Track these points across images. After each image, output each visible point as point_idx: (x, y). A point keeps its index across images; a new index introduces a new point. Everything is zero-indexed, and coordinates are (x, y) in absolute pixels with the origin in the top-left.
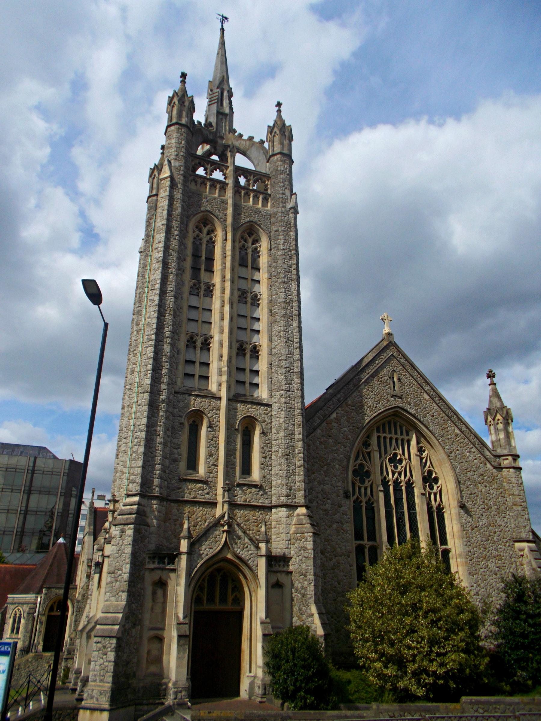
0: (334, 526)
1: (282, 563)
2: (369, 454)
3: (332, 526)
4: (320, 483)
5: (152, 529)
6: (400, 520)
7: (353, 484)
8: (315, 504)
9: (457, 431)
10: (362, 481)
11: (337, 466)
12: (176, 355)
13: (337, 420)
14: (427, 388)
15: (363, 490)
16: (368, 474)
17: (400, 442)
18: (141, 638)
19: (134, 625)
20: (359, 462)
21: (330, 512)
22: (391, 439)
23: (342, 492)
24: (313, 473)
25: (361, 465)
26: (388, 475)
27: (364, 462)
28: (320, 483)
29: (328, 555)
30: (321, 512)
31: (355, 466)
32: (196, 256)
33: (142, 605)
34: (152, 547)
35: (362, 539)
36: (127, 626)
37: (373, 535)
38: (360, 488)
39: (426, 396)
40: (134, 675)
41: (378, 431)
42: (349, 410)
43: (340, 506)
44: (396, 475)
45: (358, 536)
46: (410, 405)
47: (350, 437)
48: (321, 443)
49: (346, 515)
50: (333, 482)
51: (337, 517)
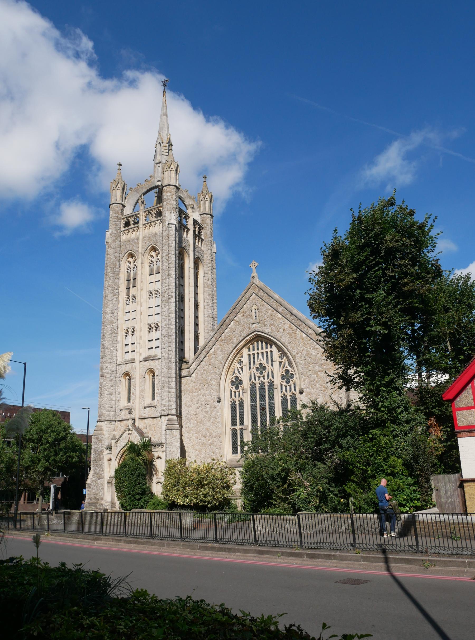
0: (212, 420)
1: (161, 447)
2: (242, 368)
3: (210, 421)
4: (203, 396)
5: (106, 436)
6: (263, 408)
7: (231, 391)
8: (200, 408)
9: (304, 335)
10: (237, 388)
11: (214, 383)
12: (115, 345)
13: (215, 353)
14: (281, 309)
15: (237, 393)
16: (241, 382)
17: (265, 354)
18: (104, 483)
19: (99, 479)
20: (234, 375)
21: (209, 412)
22: (258, 354)
23: (216, 398)
24: (200, 390)
25: (237, 377)
26: (255, 380)
27: (238, 375)
28: (203, 396)
29: (207, 438)
30: (204, 413)
31: (232, 379)
32: (128, 280)
33: (103, 470)
34: (106, 444)
35: (236, 425)
36: (94, 479)
37: (242, 422)
38: (235, 392)
39: (280, 316)
40: (102, 499)
41: (249, 351)
42: (223, 344)
43: (215, 407)
44: (262, 378)
45: (234, 423)
46: (265, 326)
47: (222, 361)
48: (204, 370)
49: (218, 412)
50: (211, 393)
51: (213, 414)
